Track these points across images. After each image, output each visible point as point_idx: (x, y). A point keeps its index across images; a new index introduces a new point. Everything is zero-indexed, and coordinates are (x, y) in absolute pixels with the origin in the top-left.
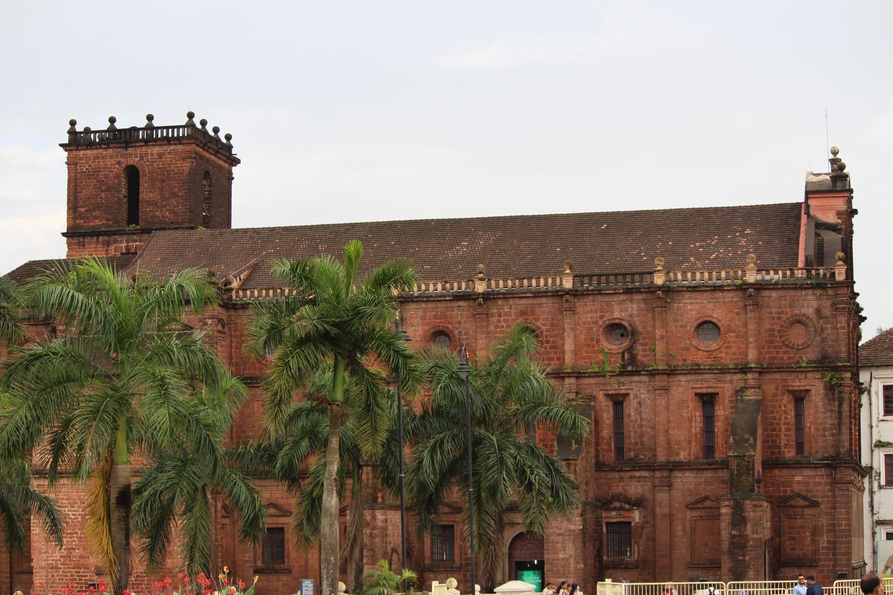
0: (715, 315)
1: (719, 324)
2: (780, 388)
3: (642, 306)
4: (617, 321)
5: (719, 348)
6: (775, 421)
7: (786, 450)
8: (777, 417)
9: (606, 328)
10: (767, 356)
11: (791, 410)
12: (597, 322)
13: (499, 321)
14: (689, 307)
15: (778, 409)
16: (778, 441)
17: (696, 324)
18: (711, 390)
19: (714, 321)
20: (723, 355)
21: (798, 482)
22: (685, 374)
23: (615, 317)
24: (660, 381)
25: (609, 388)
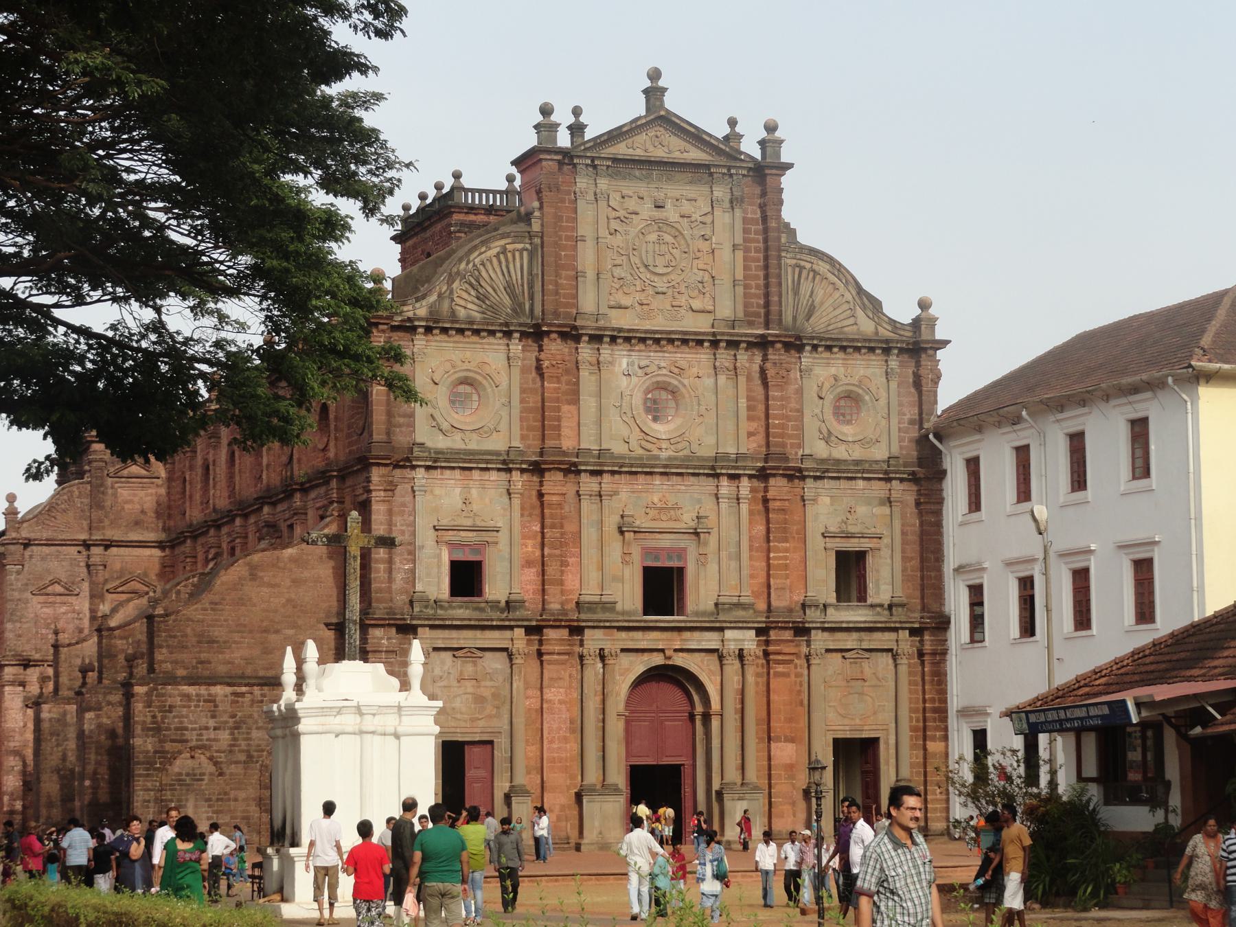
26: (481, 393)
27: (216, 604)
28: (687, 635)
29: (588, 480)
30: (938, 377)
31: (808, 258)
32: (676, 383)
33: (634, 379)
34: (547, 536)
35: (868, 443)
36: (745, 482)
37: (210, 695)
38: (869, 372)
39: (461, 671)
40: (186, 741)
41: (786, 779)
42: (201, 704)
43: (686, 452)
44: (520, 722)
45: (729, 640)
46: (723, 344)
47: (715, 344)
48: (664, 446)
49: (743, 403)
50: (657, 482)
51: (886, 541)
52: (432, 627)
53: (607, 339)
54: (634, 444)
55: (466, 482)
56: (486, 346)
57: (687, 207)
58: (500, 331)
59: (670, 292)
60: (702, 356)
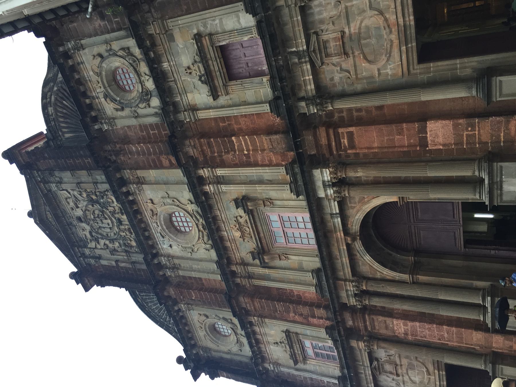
28: (330, 225)
31: (53, 123)
32: (162, 216)
35: (134, 61)
36: (201, 172)
39: (391, 373)
41: (473, 129)
43: (199, 210)
45: (327, 195)
46: (124, 189)
47: (128, 193)
48: (201, 227)
50: (226, 233)
51: (202, 29)
53: (156, 261)
55: (265, 343)
56: (190, 319)
57: (72, 204)
59: (117, 216)
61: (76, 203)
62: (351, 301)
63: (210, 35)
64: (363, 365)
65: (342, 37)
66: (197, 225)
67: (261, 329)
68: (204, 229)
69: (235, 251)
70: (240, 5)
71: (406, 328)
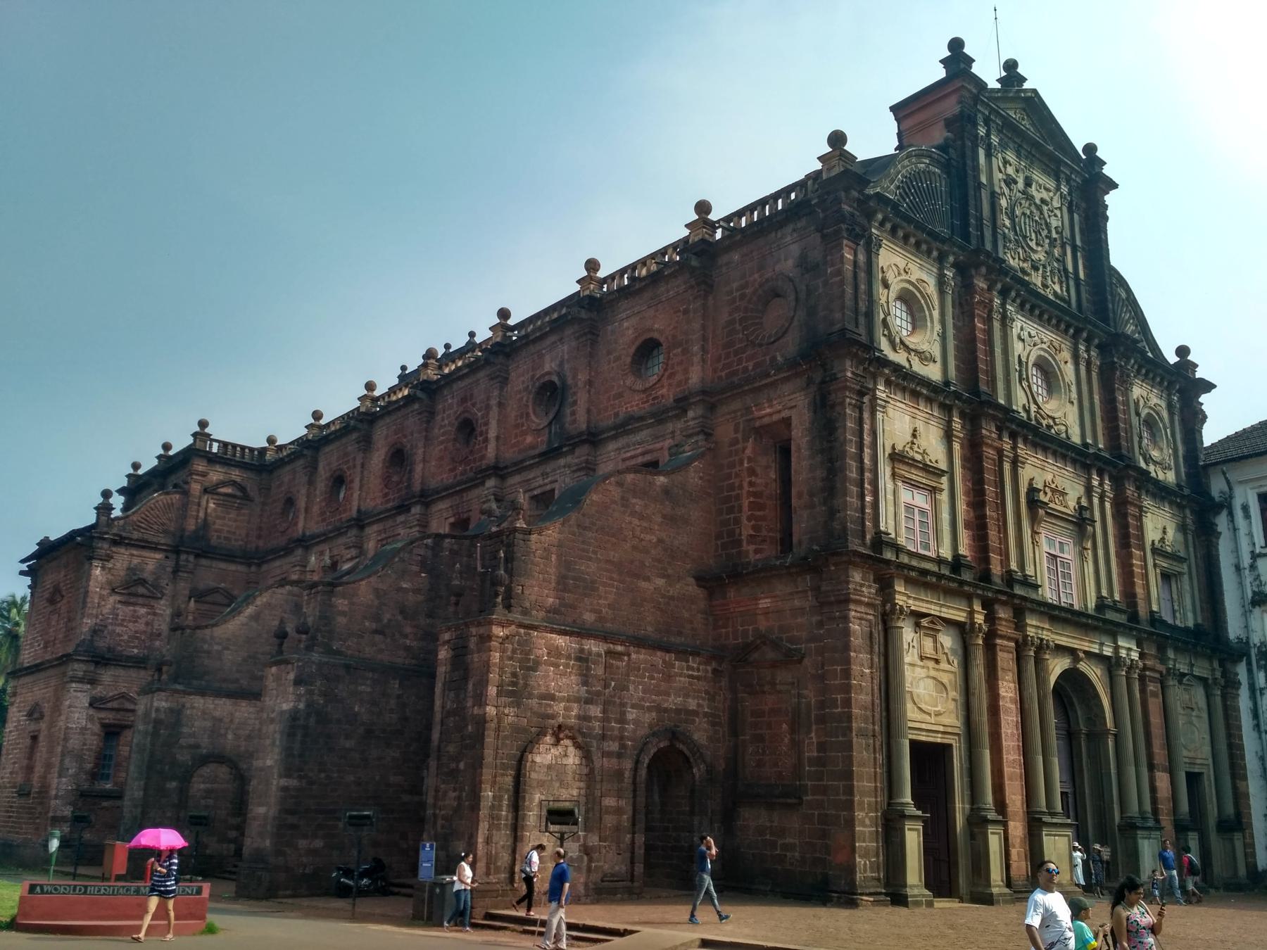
0: (656, 326)
1: (662, 340)
2: (741, 426)
3: (574, 344)
4: (547, 378)
5: (659, 381)
6: (733, 493)
7: (751, 548)
8: (737, 485)
9: (538, 393)
10: (723, 374)
11: (767, 467)
12: (528, 386)
13: (443, 420)
14: (626, 324)
15: (738, 468)
16: (737, 531)
17: (632, 350)
18: (648, 458)
19: (656, 335)
20: (664, 391)
21: (766, 612)
22: (615, 437)
23: (546, 370)
24: (583, 452)
25: (533, 486)
26: (917, 315)
27: (585, 528)
29: (1008, 440)
30: (1204, 418)
33: (1028, 348)
34: (987, 492)
37: (582, 650)
38: (1159, 402)
40: (553, 717)
42: (572, 662)
44: (983, 719)
45: (1123, 647)
46: (1085, 335)
49: (1096, 397)
50: (1051, 461)
52: (909, 581)
53: (1013, 294)
54: (1033, 414)
58: (938, 249)
59: (1041, 268)
60: (1068, 343)
61: (1047, 205)
62: (1033, 630)
63: (1184, 574)
64: (942, 606)
65: (1192, 709)
66: (1053, 419)
67: (936, 420)
68: (1049, 427)
69: (1033, 459)
70: (1200, 621)
71: (1008, 700)
